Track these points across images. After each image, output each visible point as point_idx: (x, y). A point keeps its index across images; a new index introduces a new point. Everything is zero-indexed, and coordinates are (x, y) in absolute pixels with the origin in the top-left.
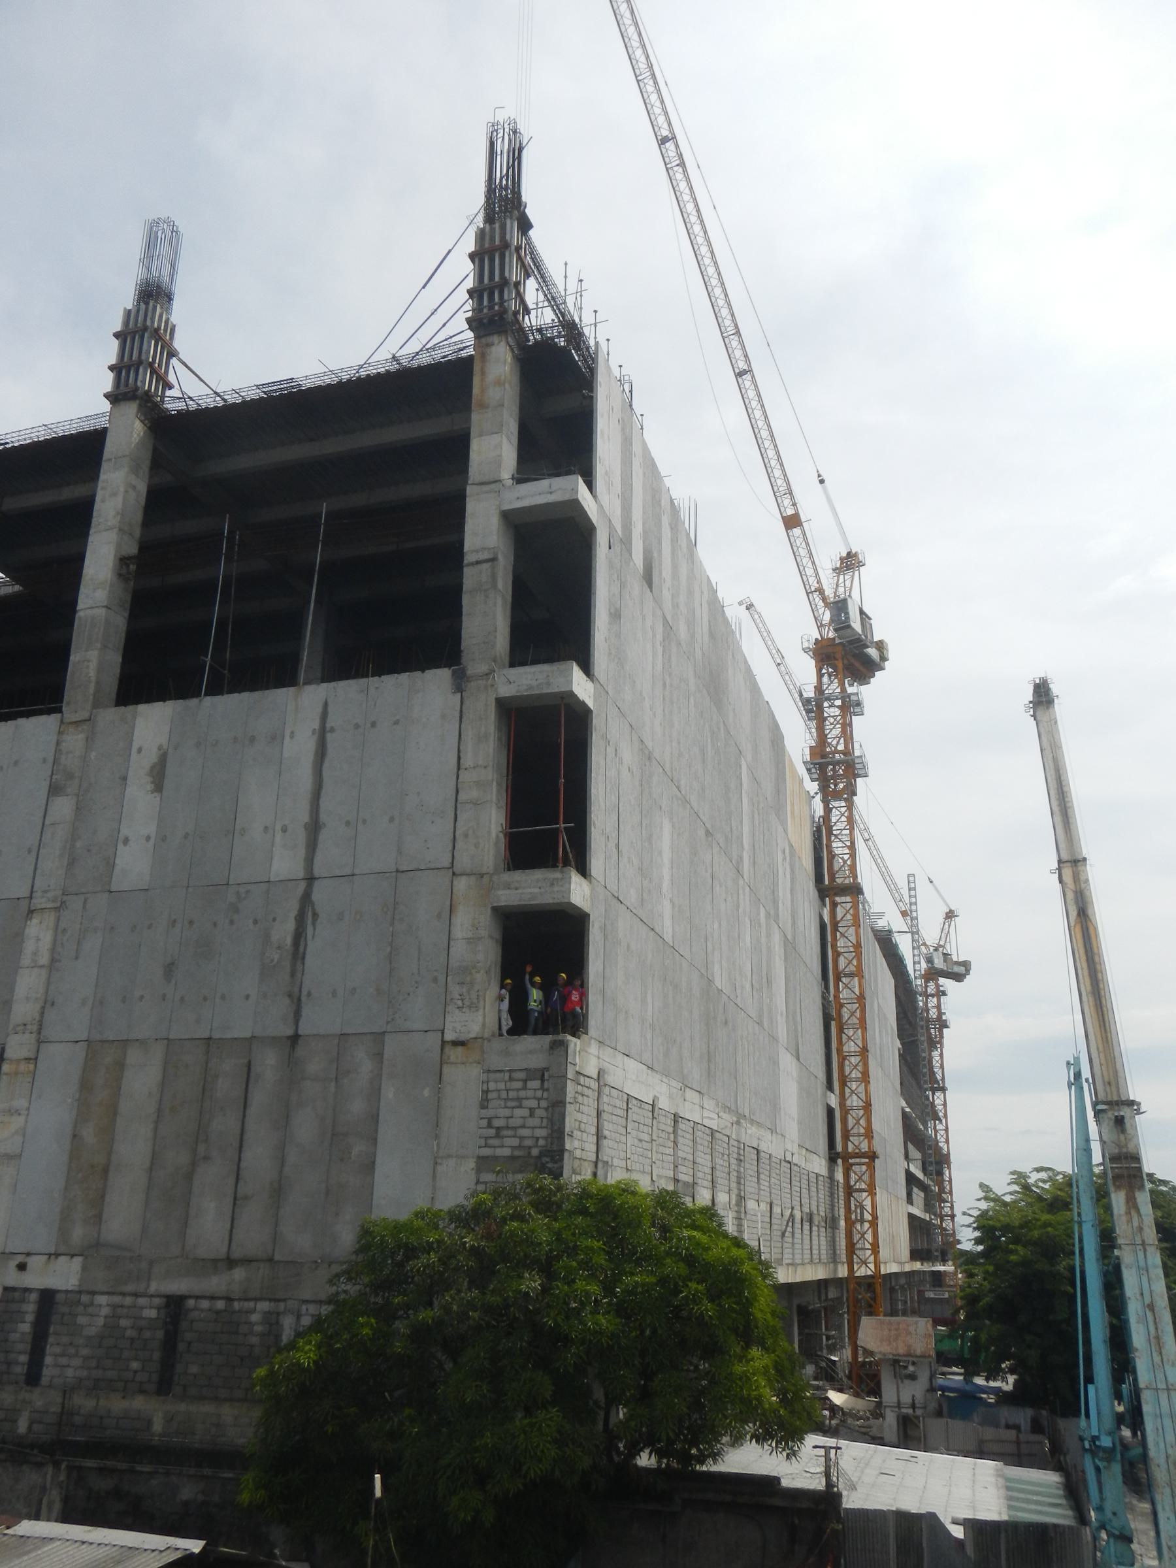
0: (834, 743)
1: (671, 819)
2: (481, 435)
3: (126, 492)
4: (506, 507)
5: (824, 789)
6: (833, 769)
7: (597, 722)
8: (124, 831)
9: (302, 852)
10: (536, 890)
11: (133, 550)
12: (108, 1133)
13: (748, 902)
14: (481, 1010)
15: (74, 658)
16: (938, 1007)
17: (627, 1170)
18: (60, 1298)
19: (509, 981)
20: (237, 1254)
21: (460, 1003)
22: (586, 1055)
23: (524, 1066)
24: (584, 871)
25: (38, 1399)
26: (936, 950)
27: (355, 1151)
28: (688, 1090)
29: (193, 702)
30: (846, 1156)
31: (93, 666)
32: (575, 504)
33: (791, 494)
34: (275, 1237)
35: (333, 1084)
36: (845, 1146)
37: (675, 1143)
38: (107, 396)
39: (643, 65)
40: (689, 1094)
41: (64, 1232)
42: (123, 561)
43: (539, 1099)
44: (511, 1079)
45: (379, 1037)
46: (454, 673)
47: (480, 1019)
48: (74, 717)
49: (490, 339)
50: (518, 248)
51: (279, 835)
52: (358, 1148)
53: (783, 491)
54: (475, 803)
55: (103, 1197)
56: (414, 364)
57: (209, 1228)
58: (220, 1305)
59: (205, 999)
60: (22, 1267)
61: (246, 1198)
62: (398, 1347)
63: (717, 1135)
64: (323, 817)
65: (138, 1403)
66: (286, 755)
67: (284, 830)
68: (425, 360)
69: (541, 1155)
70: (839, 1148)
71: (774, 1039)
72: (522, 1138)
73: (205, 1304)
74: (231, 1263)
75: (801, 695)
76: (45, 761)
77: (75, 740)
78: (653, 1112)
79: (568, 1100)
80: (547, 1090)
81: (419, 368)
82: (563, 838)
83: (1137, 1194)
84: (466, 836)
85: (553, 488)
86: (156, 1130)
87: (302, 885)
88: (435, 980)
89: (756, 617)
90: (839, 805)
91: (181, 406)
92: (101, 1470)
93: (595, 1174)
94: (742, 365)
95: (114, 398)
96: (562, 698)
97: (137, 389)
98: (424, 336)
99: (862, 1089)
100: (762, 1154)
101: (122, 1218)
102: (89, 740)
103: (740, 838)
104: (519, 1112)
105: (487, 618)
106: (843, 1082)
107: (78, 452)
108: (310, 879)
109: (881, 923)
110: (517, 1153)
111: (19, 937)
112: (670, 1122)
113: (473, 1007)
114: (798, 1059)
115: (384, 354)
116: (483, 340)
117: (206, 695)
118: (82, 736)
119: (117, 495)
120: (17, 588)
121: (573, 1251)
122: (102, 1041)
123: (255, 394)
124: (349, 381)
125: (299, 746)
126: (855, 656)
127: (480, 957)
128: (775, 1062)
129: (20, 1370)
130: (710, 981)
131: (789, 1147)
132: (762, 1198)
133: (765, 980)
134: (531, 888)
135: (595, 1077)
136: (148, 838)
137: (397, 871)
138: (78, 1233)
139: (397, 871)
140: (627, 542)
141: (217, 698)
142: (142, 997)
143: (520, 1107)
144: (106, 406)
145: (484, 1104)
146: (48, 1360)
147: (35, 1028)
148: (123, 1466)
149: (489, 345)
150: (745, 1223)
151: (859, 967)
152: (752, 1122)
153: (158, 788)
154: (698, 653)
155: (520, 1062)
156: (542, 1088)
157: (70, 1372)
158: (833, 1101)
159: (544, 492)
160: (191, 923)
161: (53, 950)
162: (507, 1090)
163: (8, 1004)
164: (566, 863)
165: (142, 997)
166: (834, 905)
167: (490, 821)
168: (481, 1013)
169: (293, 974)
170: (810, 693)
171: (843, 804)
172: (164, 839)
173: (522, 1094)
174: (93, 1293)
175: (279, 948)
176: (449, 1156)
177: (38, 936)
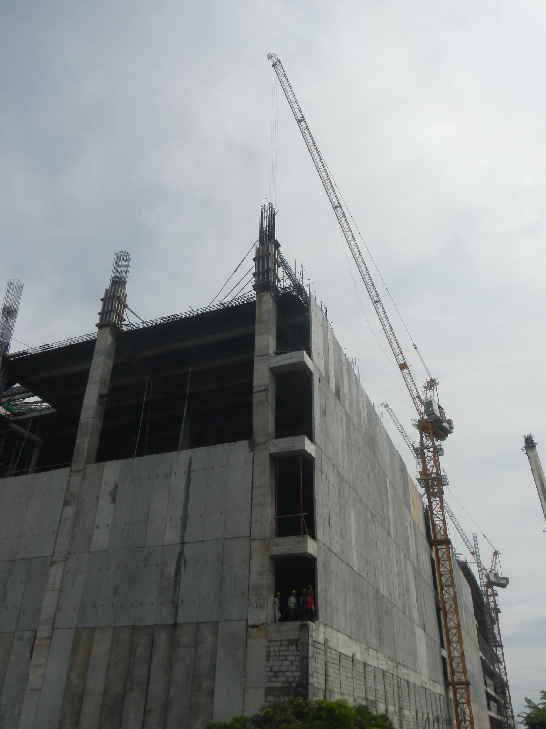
0: (431, 469)
1: (354, 509)
4: (272, 366)
5: (427, 492)
6: (432, 482)
7: (317, 463)
9: (179, 530)
10: (291, 547)
11: (105, 391)
13: (394, 550)
15: (78, 441)
16: (494, 601)
17: (341, 694)
19: (279, 593)
21: (255, 605)
22: (319, 632)
24: (313, 536)
26: (490, 571)
28: (370, 650)
29: (131, 459)
30: (454, 684)
32: (303, 363)
33: (402, 354)
35: (193, 649)
36: (453, 679)
37: (365, 678)
38: (97, 325)
39: (325, 178)
42: (101, 396)
43: (295, 656)
44: (281, 645)
45: (216, 624)
49: (263, 294)
50: (274, 255)
52: (206, 683)
53: (398, 353)
55: (80, 711)
56: (230, 305)
59: (132, 605)
63: (387, 674)
64: (189, 512)
67: (171, 520)
68: (235, 303)
69: (298, 686)
70: (450, 680)
71: (412, 621)
72: (287, 677)
75: (413, 446)
76: (62, 489)
77: (76, 479)
78: (353, 661)
79: (310, 656)
80: (299, 651)
81: (232, 307)
82: (303, 520)
84: (257, 520)
87: (180, 546)
88: (243, 594)
89: (390, 410)
90: (436, 500)
91: (128, 328)
93: (325, 697)
94: (376, 299)
97: (110, 322)
98: (234, 294)
99: (459, 647)
100: (410, 684)
103: (388, 517)
105: (264, 416)
106: (449, 643)
109: (462, 559)
110: (285, 685)
112: (362, 667)
113: (262, 607)
114: (425, 631)
115: (217, 302)
116: (260, 294)
117: (136, 456)
119: (100, 368)
120: (54, 410)
122: (83, 628)
123: (160, 322)
124: (201, 314)
125: (180, 479)
126: (438, 427)
128: (413, 633)
130: (378, 591)
131: (424, 679)
132: (412, 708)
133: (405, 590)
134: (288, 546)
135: (323, 642)
136: (108, 525)
137: (224, 539)
139: (224, 539)
140: (327, 379)
141: (142, 458)
142: (102, 605)
143: (286, 660)
144: (96, 329)
145: (268, 659)
149: (262, 296)
150: (404, 722)
151: (452, 581)
152: (404, 666)
153: (114, 501)
154: (363, 429)
156: (297, 650)
158: (445, 653)
159: (288, 359)
161: (62, 581)
162: (279, 651)
164: (305, 533)
165: (102, 605)
166: (437, 550)
167: (268, 513)
168: (265, 611)
169: (174, 592)
170: (417, 445)
171: (438, 499)
173: (287, 653)
175: (168, 578)
176: (251, 687)
177: (55, 574)
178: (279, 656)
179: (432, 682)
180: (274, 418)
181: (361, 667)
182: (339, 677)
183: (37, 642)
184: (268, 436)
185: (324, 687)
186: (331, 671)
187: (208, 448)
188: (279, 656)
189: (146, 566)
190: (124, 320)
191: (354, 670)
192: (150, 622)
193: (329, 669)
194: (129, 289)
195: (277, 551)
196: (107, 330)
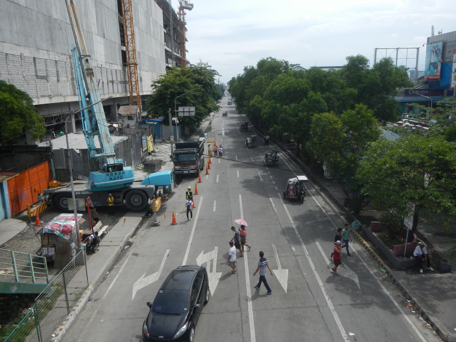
16: (183, 18)
37: (35, 65)
40: (40, 51)
83: (93, 78)
114: (104, 37)
133: (83, 14)
179: (108, 64)
181: (31, 60)
182: (6, 66)
191: (23, 62)
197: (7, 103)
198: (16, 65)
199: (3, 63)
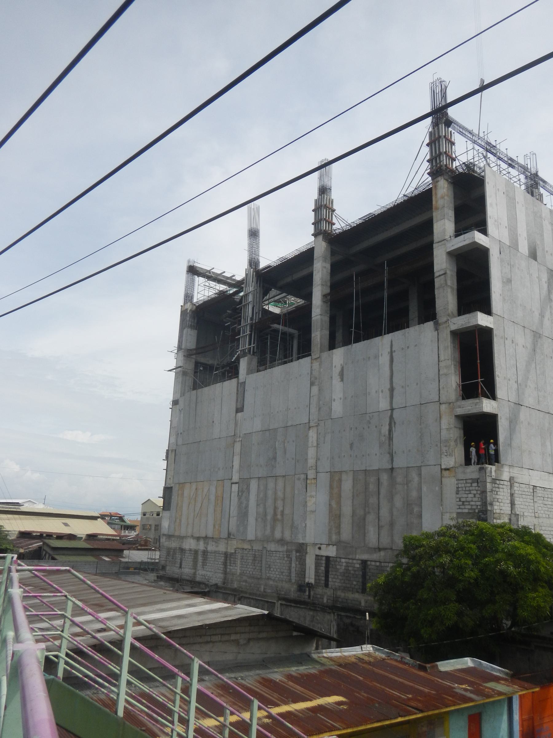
2: (437, 221)
3: (322, 270)
4: (448, 250)
7: (495, 332)
8: (334, 397)
9: (388, 399)
10: (470, 408)
11: (328, 290)
12: (339, 503)
14: (454, 457)
15: (313, 335)
17: (535, 517)
18: (331, 559)
20: (381, 547)
21: (446, 454)
23: (470, 478)
24: (493, 396)
25: (329, 592)
27: (415, 510)
29: (350, 346)
31: (319, 337)
32: (475, 243)
34: (392, 541)
41: (330, 538)
42: (325, 296)
43: (477, 490)
44: (466, 483)
46: (434, 323)
47: (454, 460)
48: (316, 357)
51: (381, 393)
52: (416, 509)
54: (446, 375)
55: (340, 525)
56: (413, 195)
57: (372, 538)
58: (378, 564)
60: (320, 548)
61: (382, 527)
62: (407, 579)
64: (394, 385)
65: (357, 596)
66: (380, 363)
67: (382, 392)
68: (416, 192)
69: (479, 512)
72: (472, 505)
73: (373, 563)
74: (380, 549)
77: (316, 365)
79: (488, 490)
81: (415, 196)
84: (443, 388)
85: (465, 238)
86: (353, 502)
87: (390, 411)
88: (437, 445)
92: (347, 616)
95: (315, 235)
96: (476, 327)
97: (321, 230)
98: (414, 185)
101: (346, 534)
102: (320, 365)
104: (470, 495)
105: (446, 297)
107: (305, 258)
108: (392, 409)
110: (470, 511)
111: (307, 436)
113: (451, 455)
116: (435, 180)
118: (318, 363)
119: (320, 271)
121: (462, 549)
123: (358, 222)
125: (384, 359)
127: (452, 436)
129: (323, 582)
135: (508, 479)
136: (341, 399)
138: (334, 537)
140: (514, 245)
143: (470, 493)
144: (313, 238)
146: (330, 579)
147: (315, 468)
148: (352, 615)
149: (437, 182)
153: (342, 380)
155: (469, 476)
157: (337, 584)
160: (356, 428)
161: (317, 441)
163: (306, 460)
167: (453, 380)
172: (345, 398)
173: (471, 488)
174: (340, 558)
177: (312, 435)
178: (465, 491)
180: (456, 297)
183: (308, 482)
184: (449, 315)
185: (510, 513)
186: (517, 501)
187: (403, 330)
188: (465, 491)
189: (369, 427)
190: (334, 224)
192: (376, 468)
193: (517, 499)
194: (335, 195)
195: (460, 411)
196: (320, 238)
197: (530, 562)
198: (546, 503)
199: (529, 500)
